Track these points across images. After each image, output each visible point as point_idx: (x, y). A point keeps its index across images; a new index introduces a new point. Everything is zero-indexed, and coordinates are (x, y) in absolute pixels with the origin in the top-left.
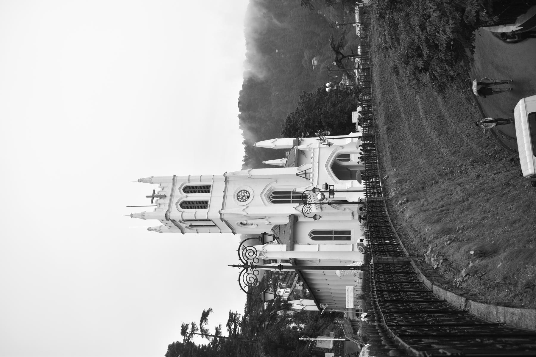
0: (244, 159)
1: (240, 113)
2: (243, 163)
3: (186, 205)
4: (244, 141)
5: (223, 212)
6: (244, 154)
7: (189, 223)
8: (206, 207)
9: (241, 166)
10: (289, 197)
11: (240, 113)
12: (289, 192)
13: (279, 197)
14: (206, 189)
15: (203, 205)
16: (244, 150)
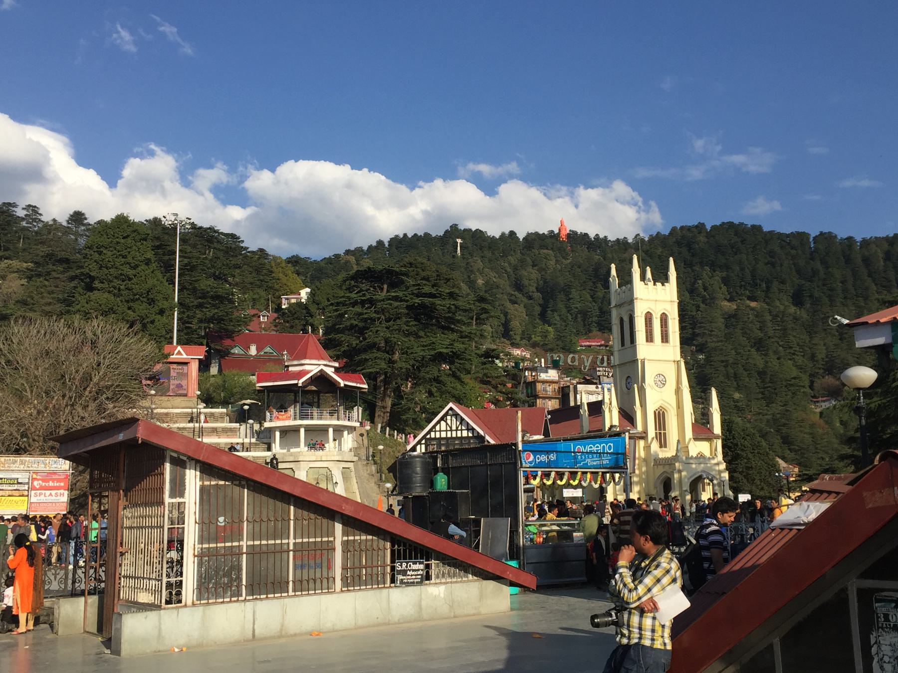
0: (601, 236)
1: (708, 228)
2: (592, 236)
3: (649, 318)
4: (642, 240)
5: (646, 363)
6: (612, 238)
7: (626, 319)
8: (647, 341)
9: (584, 232)
10: (660, 429)
11: (708, 228)
12: (665, 429)
13: (660, 417)
14: (665, 338)
15: (650, 338)
16: (621, 237)
